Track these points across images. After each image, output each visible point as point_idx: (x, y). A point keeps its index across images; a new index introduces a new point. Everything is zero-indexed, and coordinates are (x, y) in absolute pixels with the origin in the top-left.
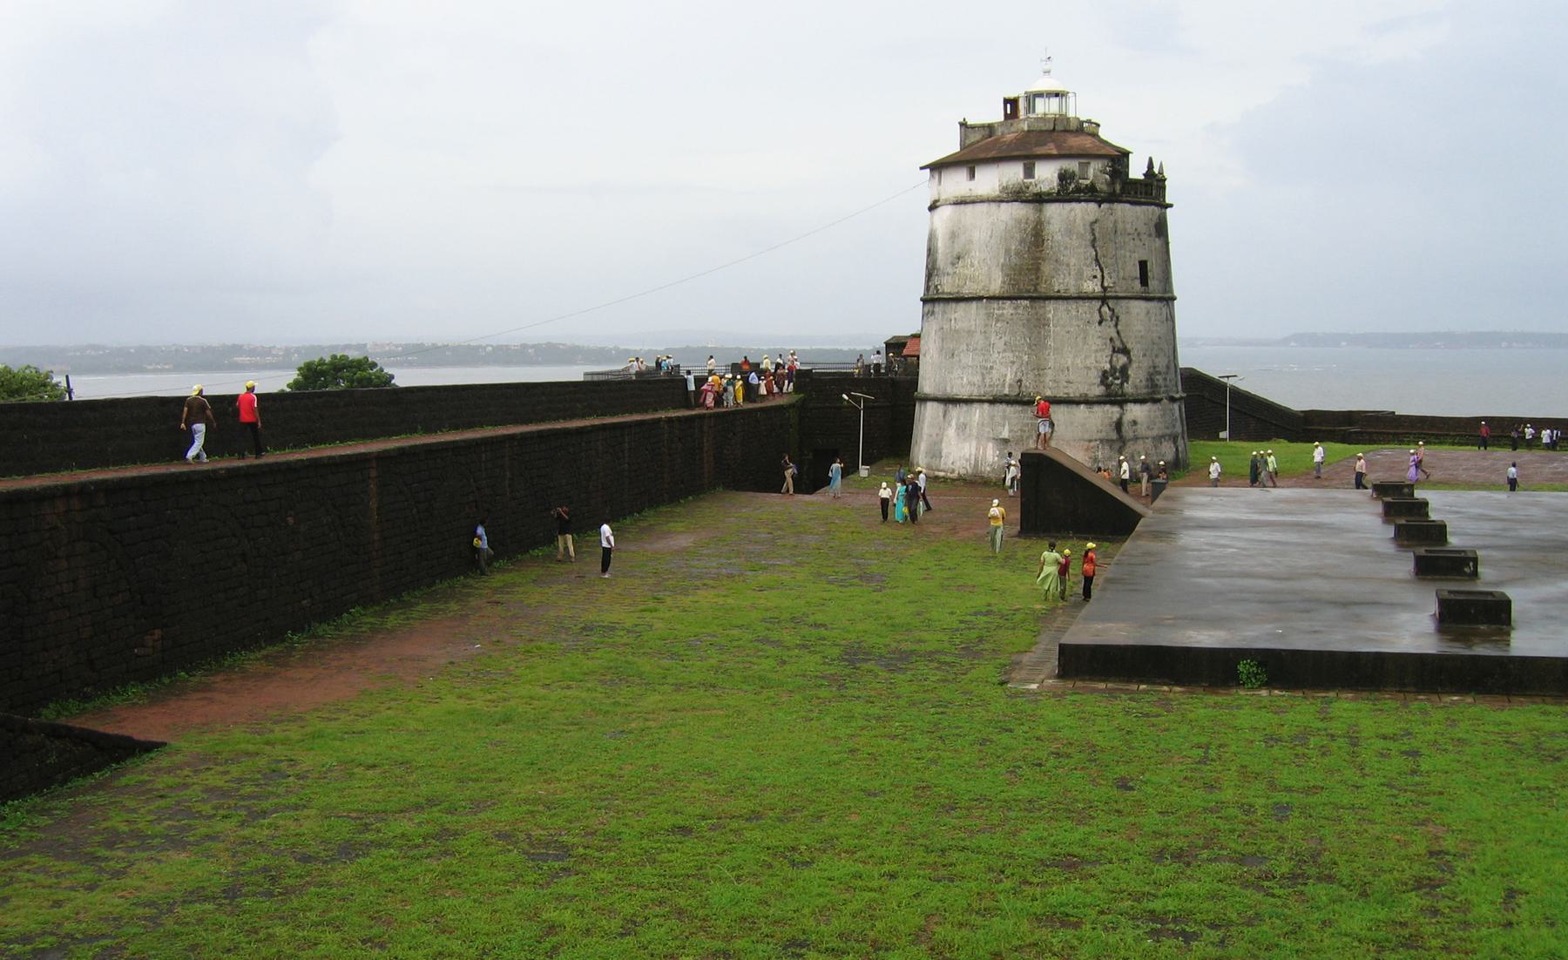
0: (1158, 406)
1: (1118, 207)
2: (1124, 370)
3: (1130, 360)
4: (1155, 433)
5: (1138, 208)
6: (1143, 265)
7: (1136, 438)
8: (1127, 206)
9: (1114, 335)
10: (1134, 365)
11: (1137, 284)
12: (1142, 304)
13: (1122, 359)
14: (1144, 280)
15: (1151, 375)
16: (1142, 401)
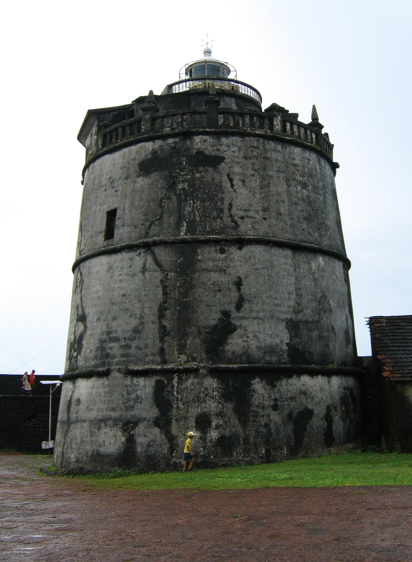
0: (104, 381)
1: (98, 162)
2: (81, 338)
3: (86, 327)
4: (93, 415)
5: (117, 155)
6: (112, 215)
7: (77, 421)
8: (107, 157)
9: (79, 301)
10: (89, 332)
11: (101, 238)
12: (104, 260)
13: (81, 326)
14: (109, 233)
15: (102, 342)
16: (88, 375)
